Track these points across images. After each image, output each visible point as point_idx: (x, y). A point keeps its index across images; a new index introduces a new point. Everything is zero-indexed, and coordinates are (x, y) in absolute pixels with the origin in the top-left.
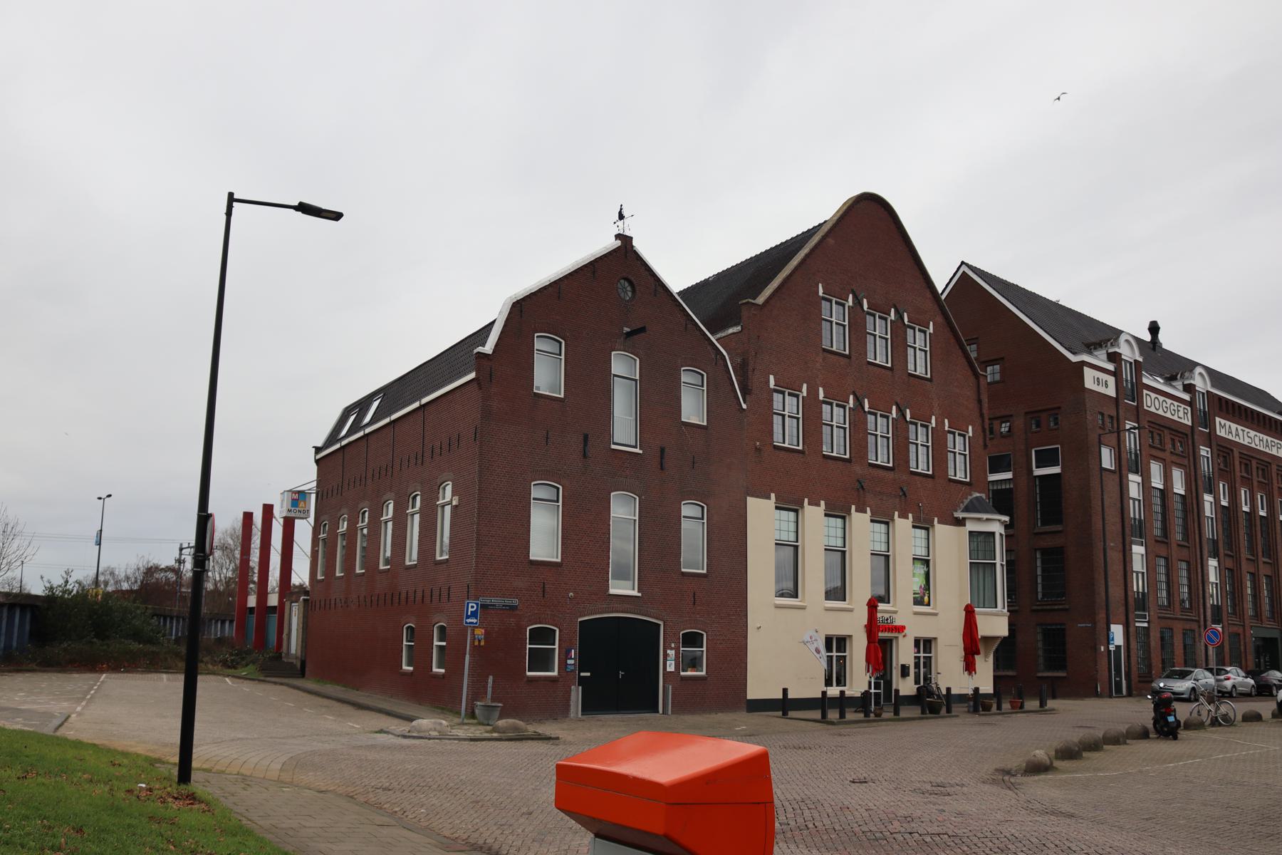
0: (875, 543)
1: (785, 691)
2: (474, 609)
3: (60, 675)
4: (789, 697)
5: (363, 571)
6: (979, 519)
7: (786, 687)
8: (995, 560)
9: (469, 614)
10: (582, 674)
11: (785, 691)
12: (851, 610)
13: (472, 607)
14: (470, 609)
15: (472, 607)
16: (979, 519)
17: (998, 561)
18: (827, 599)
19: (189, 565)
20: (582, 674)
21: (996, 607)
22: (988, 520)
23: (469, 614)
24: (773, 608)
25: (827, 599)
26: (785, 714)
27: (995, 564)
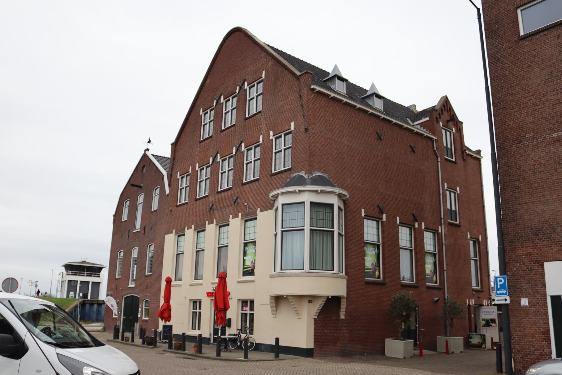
0: (326, 213)
1: (277, 340)
2: (502, 283)
3: (350, 362)
4: (280, 344)
5: (120, 277)
6: (294, 192)
7: (278, 337)
8: (333, 228)
9: (499, 287)
10: (215, 336)
11: (277, 340)
12: (201, 284)
13: (501, 281)
14: (499, 283)
15: (501, 281)
16: (294, 192)
17: (336, 229)
18: (243, 275)
19: (246, 267)
20: (215, 336)
21: (333, 270)
22: (300, 192)
23: (499, 287)
24: (236, 283)
25: (243, 275)
26: (277, 356)
27: (333, 232)
